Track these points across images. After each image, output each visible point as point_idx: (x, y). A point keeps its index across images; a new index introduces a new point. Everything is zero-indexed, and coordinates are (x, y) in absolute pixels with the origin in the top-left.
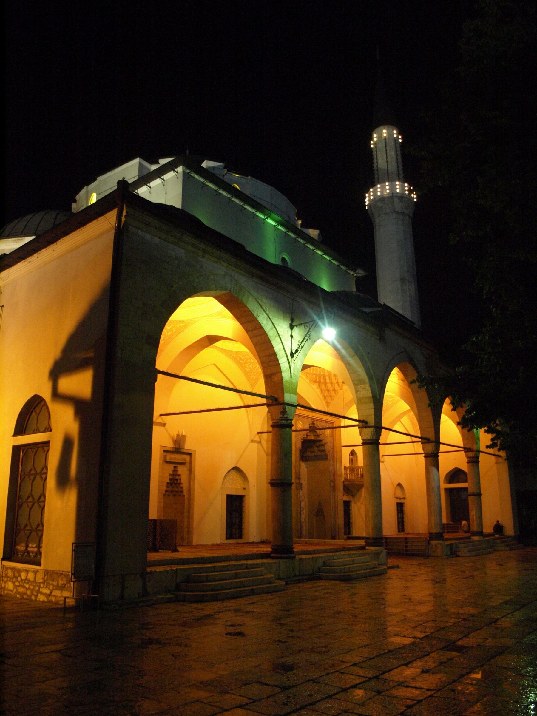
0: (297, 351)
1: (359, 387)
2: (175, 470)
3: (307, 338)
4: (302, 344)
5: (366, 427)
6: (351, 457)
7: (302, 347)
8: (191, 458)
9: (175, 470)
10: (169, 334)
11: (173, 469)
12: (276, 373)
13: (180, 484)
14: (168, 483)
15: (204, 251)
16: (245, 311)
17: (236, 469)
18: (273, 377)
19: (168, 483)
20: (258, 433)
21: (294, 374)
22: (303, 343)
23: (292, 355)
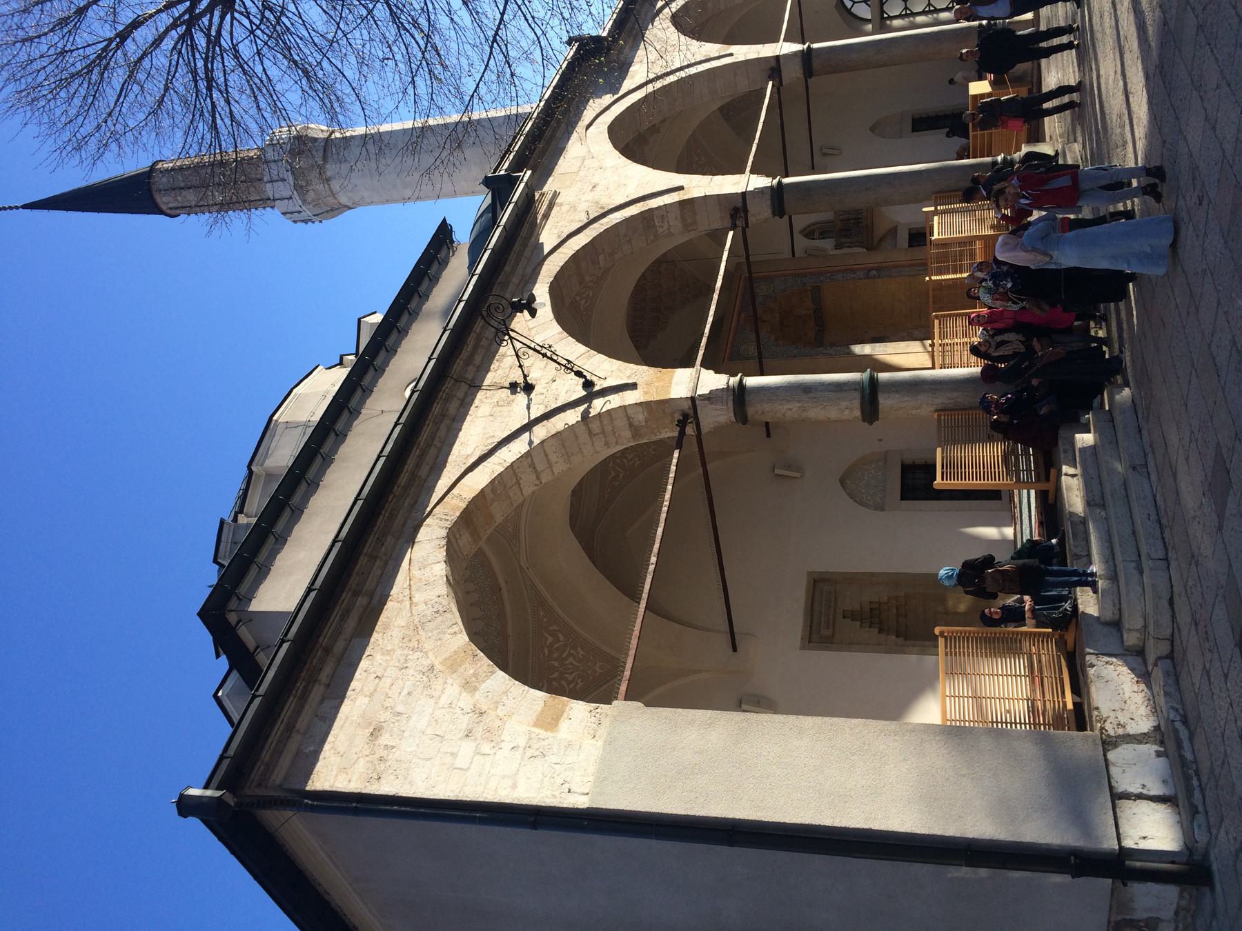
0: (579, 374)
1: (660, 230)
2: (852, 616)
3: (549, 354)
4: (564, 362)
5: (745, 210)
6: (816, 235)
7: (569, 362)
8: (823, 580)
9: (852, 616)
10: (561, 638)
11: (848, 620)
12: (629, 418)
13: (880, 603)
14: (880, 631)
15: (356, 594)
16: (493, 491)
17: (842, 482)
18: (636, 423)
19: (880, 631)
20: (768, 435)
21: (629, 377)
22: (560, 360)
23: (588, 384)
